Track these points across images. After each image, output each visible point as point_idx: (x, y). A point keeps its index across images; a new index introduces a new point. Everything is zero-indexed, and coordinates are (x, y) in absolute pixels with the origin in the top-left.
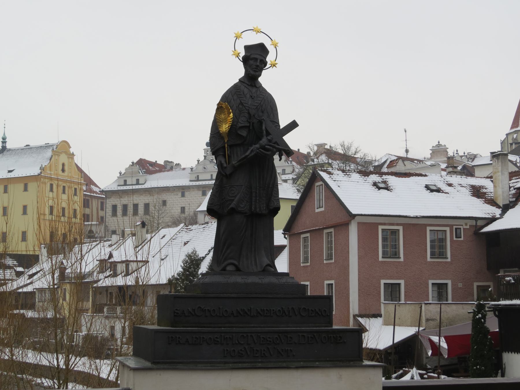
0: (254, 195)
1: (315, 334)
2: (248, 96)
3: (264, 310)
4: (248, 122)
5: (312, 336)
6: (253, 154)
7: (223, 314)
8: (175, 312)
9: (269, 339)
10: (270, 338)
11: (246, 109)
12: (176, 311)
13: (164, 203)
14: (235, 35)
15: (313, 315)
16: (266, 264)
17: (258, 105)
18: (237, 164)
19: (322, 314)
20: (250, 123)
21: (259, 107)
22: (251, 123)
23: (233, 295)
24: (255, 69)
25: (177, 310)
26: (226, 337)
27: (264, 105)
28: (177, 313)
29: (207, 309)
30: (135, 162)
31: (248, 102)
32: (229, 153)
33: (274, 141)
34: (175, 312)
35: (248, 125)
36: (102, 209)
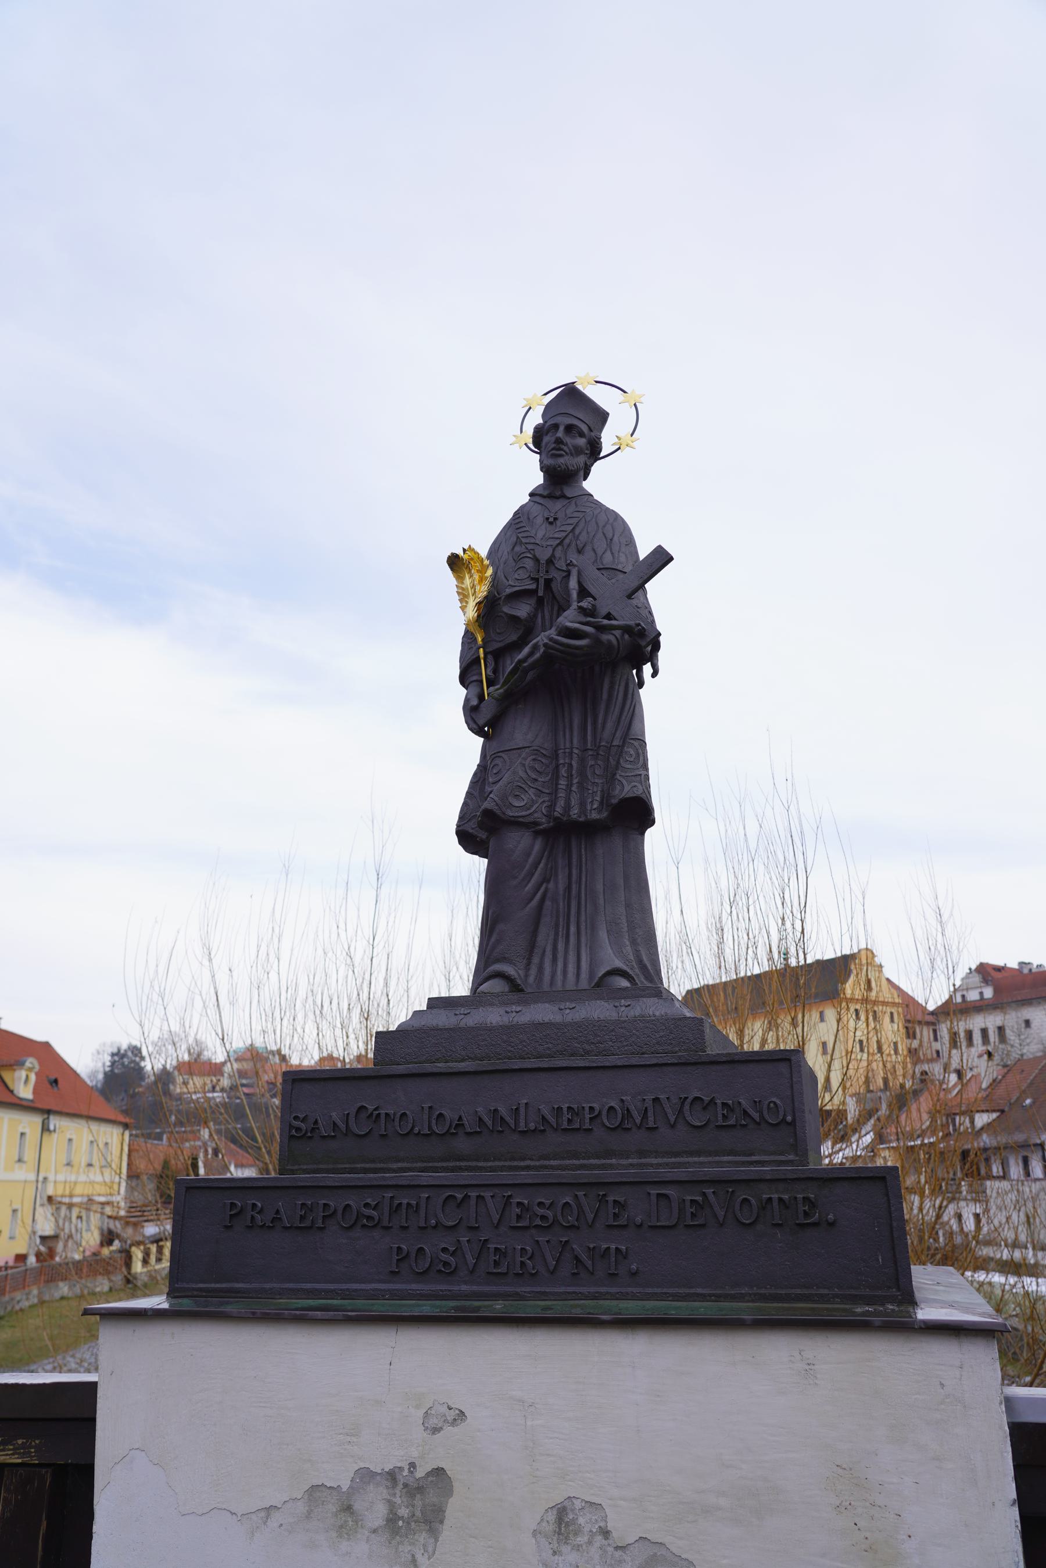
0: (563, 771)
1: (709, 1191)
2: (540, 520)
3: (560, 1109)
4: (532, 579)
5: (699, 1198)
6: (537, 655)
7: (430, 1128)
8: (291, 1127)
9: (541, 1211)
10: (540, 1204)
11: (527, 549)
12: (296, 1123)
13: (1028, 1023)
14: (524, 403)
15: (732, 1122)
16: (608, 968)
17: (566, 536)
18: (501, 691)
19: (762, 1117)
20: (537, 580)
21: (567, 541)
22: (542, 582)
23: (462, 1066)
24: (554, 452)
25: (296, 1118)
26: (397, 1202)
27: (584, 533)
28: (298, 1129)
29: (383, 1112)
30: (974, 967)
31: (536, 535)
32: (490, 673)
33: (604, 611)
34: (291, 1127)
35: (534, 586)
36: (936, 1039)
